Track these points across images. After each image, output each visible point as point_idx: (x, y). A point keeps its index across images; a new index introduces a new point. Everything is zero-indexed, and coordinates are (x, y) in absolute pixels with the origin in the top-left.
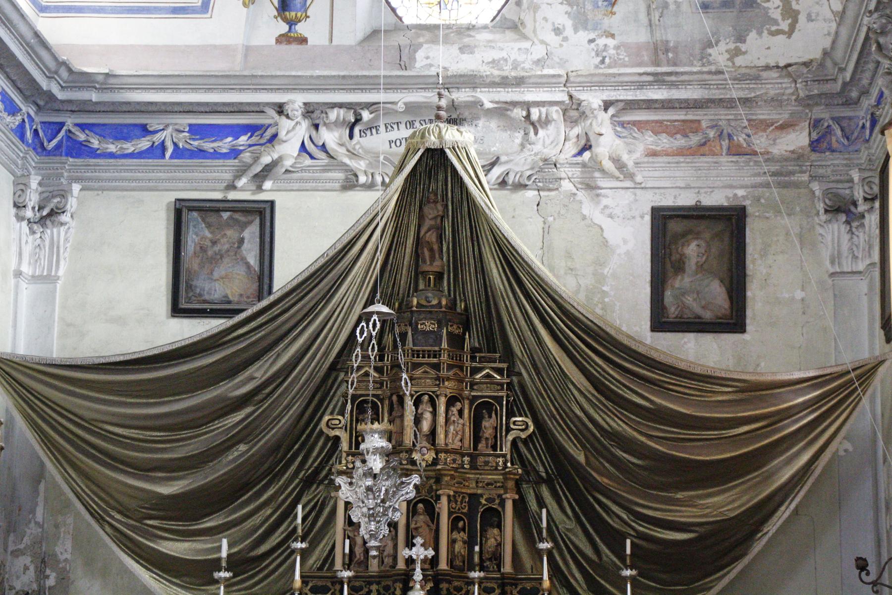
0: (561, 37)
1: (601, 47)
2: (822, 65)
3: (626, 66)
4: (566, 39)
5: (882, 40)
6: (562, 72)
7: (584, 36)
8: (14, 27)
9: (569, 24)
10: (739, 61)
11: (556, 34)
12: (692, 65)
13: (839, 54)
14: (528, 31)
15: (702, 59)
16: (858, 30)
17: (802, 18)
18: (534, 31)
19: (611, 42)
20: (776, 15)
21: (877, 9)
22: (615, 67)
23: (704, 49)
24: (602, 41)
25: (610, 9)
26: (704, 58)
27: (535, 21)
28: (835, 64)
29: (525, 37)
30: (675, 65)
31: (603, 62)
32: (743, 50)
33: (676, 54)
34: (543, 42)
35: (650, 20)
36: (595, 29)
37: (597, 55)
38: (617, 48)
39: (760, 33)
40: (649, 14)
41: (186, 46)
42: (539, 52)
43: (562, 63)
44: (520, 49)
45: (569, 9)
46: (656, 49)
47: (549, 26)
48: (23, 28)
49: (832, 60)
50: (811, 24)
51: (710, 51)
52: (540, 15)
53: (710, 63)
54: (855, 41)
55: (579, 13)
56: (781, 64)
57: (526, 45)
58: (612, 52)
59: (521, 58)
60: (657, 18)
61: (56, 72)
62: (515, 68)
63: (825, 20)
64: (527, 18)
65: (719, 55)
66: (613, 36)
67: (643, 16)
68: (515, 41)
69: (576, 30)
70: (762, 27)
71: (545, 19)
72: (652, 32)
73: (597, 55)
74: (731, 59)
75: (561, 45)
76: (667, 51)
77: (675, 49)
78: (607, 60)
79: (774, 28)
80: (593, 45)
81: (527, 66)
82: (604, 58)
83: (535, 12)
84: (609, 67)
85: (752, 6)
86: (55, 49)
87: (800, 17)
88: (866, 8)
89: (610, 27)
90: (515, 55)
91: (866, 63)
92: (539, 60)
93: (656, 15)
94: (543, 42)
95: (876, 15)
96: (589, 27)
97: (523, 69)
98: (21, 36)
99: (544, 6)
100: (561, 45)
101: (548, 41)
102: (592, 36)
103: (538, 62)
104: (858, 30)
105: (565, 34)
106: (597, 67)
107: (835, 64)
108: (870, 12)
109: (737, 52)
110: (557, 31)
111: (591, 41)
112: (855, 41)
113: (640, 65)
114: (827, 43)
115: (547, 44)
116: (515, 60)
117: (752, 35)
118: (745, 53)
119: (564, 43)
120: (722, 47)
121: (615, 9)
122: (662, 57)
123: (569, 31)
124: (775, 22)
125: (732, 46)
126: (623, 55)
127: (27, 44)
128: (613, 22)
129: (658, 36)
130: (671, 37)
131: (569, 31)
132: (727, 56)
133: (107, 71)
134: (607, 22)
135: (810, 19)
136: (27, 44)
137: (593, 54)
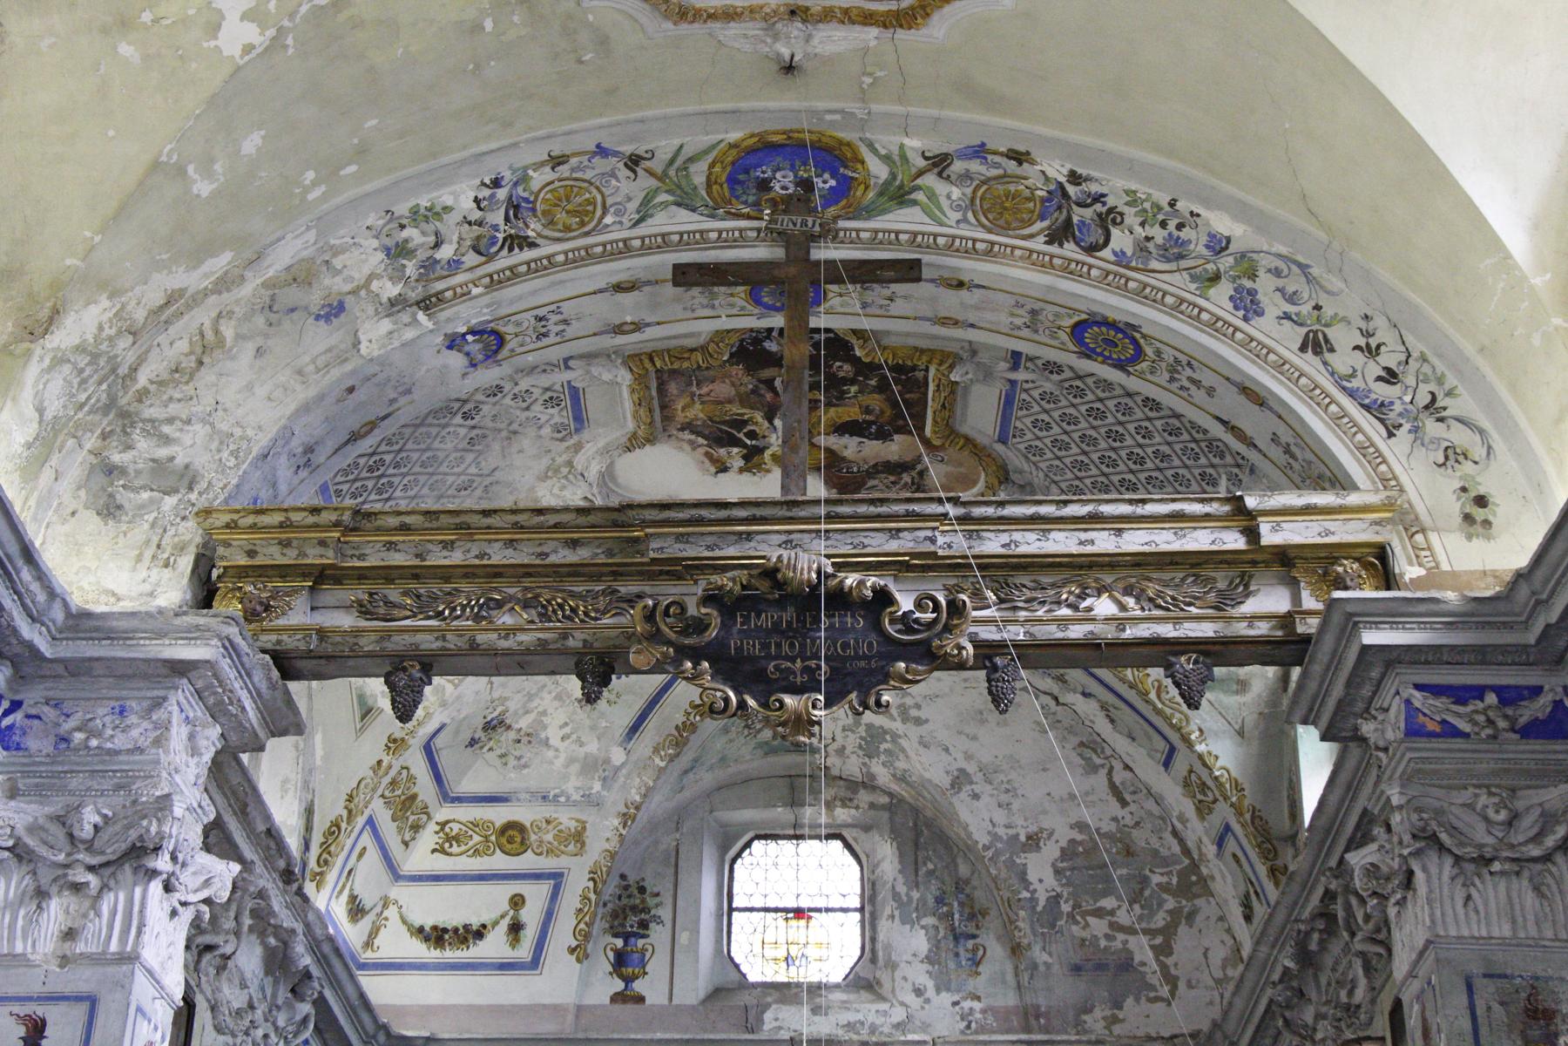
0: (921, 999)
1: (966, 1010)
2: (1210, 1037)
3: (994, 1032)
4: (928, 1001)
5: (1287, 1014)
6: (927, 1038)
7: (946, 998)
8: (341, 988)
9: (930, 984)
10: (1117, 1029)
11: (917, 996)
12: (1067, 1033)
13: (1230, 1026)
14: (886, 989)
15: (1076, 1026)
16: (1256, 1001)
17: (1182, 985)
18: (893, 991)
19: (977, 1005)
20: (1155, 980)
21: (1281, 981)
22: (983, 1033)
23: (1079, 1015)
24: (967, 1004)
25: (974, 969)
26: (1079, 1026)
27: (893, 981)
28: (1226, 1037)
29: (883, 999)
30: (1048, 1032)
31: (968, 1027)
32: (1121, 1017)
33: (1048, 1020)
34: (902, 1004)
35: (1018, 983)
36: (958, 991)
37: (962, 1019)
38: (984, 1011)
39: (1137, 1000)
40: (1017, 975)
41: (513, 1006)
42: (898, 1014)
43: (925, 1027)
44: (877, 1011)
45: (930, 968)
46: (1026, 1014)
47: (909, 986)
48: (350, 989)
49: (1223, 1032)
50: (1193, 992)
51: (1085, 1017)
52: (898, 974)
53: (1085, 1032)
54: (1251, 1013)
55: (941, 973)
56: (1167, 1034)
57: (884, 1006)
58: (978, 1016)
59: (879, 1021)
60: (1026, 979)
61: (374, 1037)
62: (872, 1032)
63: (1206, 987)
64: (884, 976)
65: (1095, 1022)
66: (978, 999)
67: (1010, 977)
68: (872, 1002)
69: (938, 990)
70: (1140, 992)
71: (905, 979)
72: (1021, 996)
73: (962, 1019)
74: (1107, 1027)
75: (923, 1008)
76: (1037, 1017)
77: (1047, 1015)
78: (973, 1025)
79: (1152, 994)
80: (957, 1008)
81: (886, 1030)
82: (970, 1022)
83: (893, 972)
84: (976, 1032)
85: (1127, 970)
86: (378, 1011)
87: (1179, 984)
88: (1268, 977)
89: (975, 988)
90: (872, 1018)
91: (1263, 1038)
92: (899, 1024)
93: (1026, 977)
94: (902, 1004)
95: (1280, 987)
96: (953, 985)
97: (881, 1033)
98: (347, 998)
99: (903, 965)
100: (923, 1008)
101: (908, 1003)
102: (956, 998)
103: (897, 1026)
104: (1256, 1001)
105: (927, 995)
106: (962, 1032)
107: (1226, 1037)
108: (1273, 983)
109: (1115, 1020)
110: (919, 992)
111: (955, 1004)
112: (1251, 1013)
113: (1008, 1032)
114: (1215, 1014)
115: (907, 1006)
116: (872, 1024)
117: (1130, 1001)
118: (1123, 1021)
119: (927, 1006)
120: (1098, 1013)
121: (980, 969)
122: (1033, 1022)
123: (931, 993)
124: (1153, 988)
125: (1108, 1013)
126: (990, 1020)
127: (351, 1007)
128: (979, 983)
129: (1029, 999)
130: (1042, 1001)
131: (931, 993)
132: (1103, 1024)
133: (428, 1034)
134: (972, 984)
135: (1190, 985)
136: (351, 1007)
137: (958, 1018)
